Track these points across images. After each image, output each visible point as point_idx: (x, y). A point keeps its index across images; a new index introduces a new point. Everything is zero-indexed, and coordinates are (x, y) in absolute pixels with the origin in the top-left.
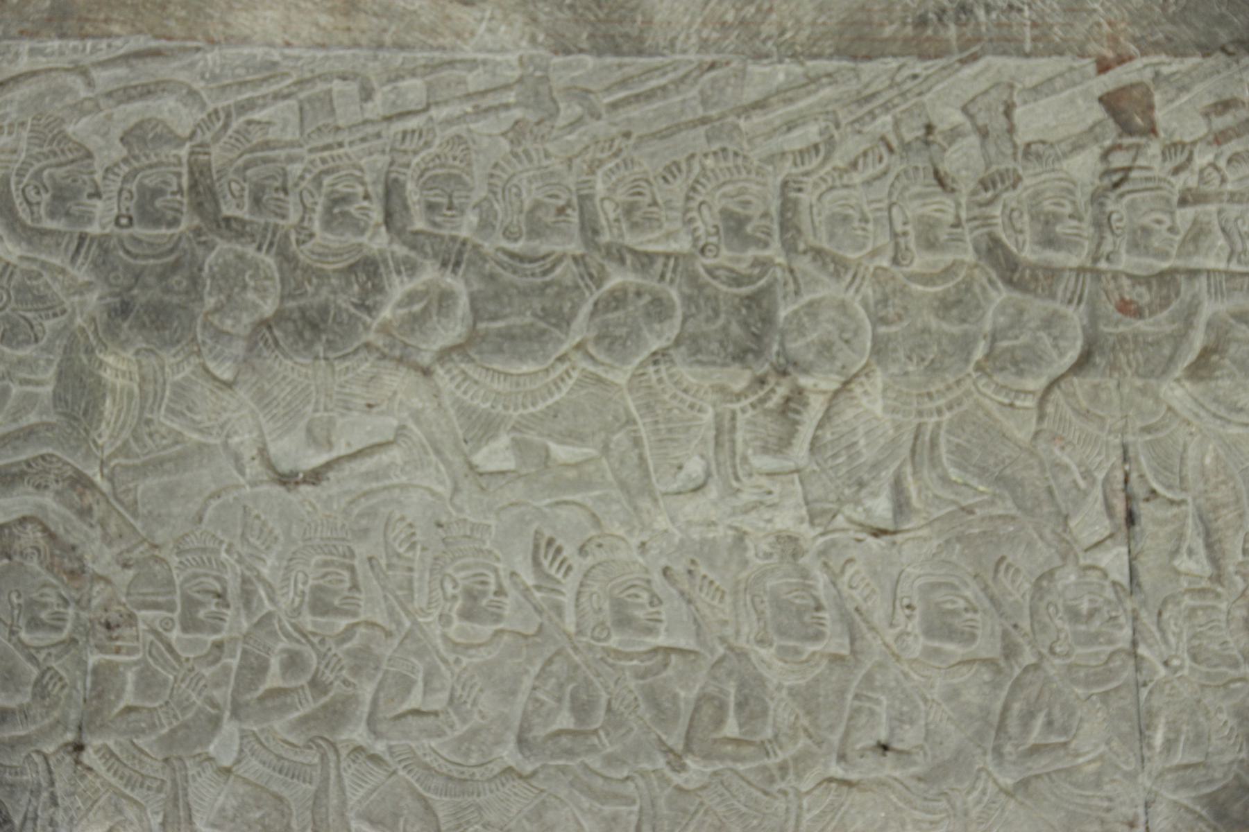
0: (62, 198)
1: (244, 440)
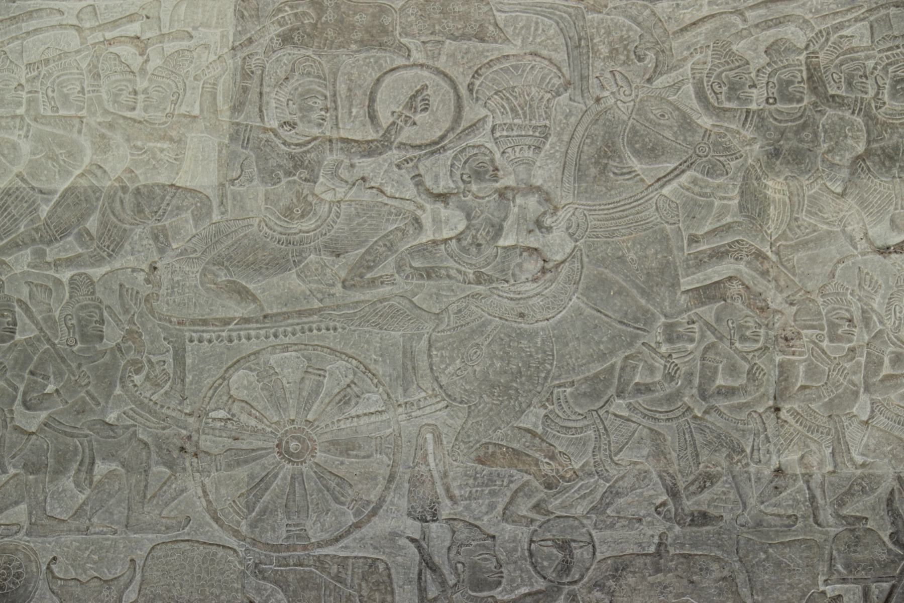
0: (734, 89)
1: (854, 228)
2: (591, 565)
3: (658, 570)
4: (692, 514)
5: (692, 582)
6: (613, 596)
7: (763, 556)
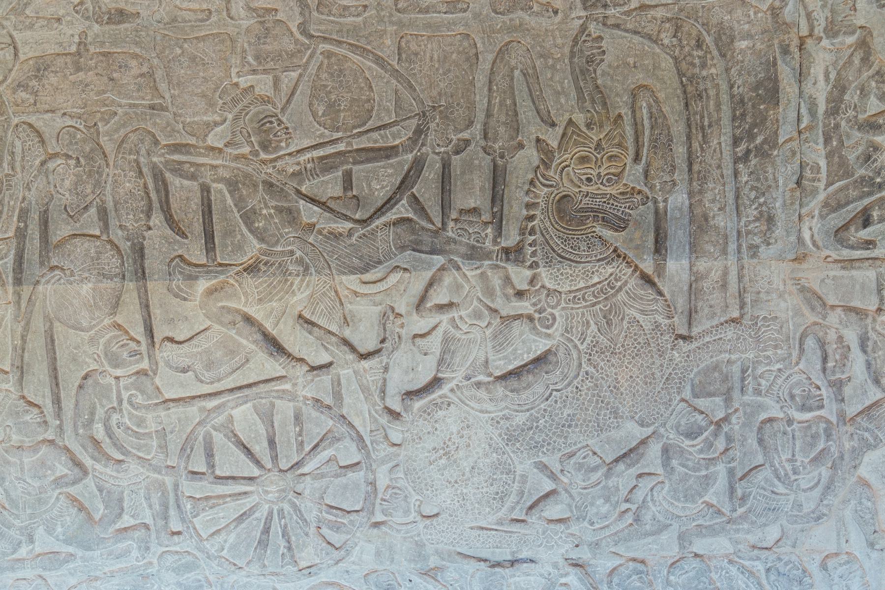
2: (14, 66)
3: (78, 69)
4: (109, 13)
5: (112, 80)
6: (37, 96)
7: (179, 51)
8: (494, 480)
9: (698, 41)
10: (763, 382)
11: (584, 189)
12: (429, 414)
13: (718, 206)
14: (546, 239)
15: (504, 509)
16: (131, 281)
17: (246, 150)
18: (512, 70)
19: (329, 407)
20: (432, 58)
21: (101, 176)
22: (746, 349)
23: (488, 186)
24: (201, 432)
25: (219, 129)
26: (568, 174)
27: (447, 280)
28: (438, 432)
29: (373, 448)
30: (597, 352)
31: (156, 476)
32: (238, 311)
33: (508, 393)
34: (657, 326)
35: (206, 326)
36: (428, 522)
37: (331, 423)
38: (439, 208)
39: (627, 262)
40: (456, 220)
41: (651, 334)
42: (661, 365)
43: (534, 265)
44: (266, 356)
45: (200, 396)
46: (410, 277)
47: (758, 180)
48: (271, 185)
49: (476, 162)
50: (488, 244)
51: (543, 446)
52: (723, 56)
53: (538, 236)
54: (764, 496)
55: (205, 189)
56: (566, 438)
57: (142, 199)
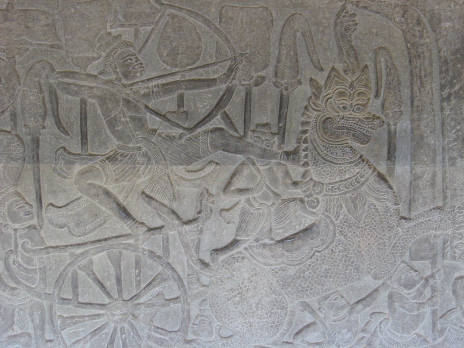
3: (6, 20)
5: (27, 27)
7: (73, 10)
8: (272, 313)
9: (418, 21)
10: (457, 251)
11: (342, 114)
12: (229, 265)
13: (430, 130)
14: (315, 147)
15: (278, 334)
16: (29, 163)
17: (113, 77)
18: (295, 32)
19: (160, 257)
20: (242, 22)
21: (15, 91)
22: (446, 228)
23: (276, 109)
24: (71, 269)
25: (95, 63)
26: (331, 103)
27: (246, 172)
28: (235, 278)
29: (189, 288)
30: (347, 226)
31: (38, 299)
32: (100, 187)
33: (284, 252)
34: (387, 210)
35: (78, 197)
36: (225, 341)
37: (160, 268)
38: (242, 122)
39: (369, 165)
40: (254, 131)
41: (383, 215)
42: (390, 237)
43: (306, 164)
44: (117, 219)
45: (71, 245)
46: (220, 169)
47: (456, 114)
48: (128, 102)
49: (269, 92)
50: (275, 148)
51: (307, 291)
52: (435, 31)
53: (308, 145)
54: (455, 330)
55: (83, 102)
56: (323, 285)
57: (41, 108)
